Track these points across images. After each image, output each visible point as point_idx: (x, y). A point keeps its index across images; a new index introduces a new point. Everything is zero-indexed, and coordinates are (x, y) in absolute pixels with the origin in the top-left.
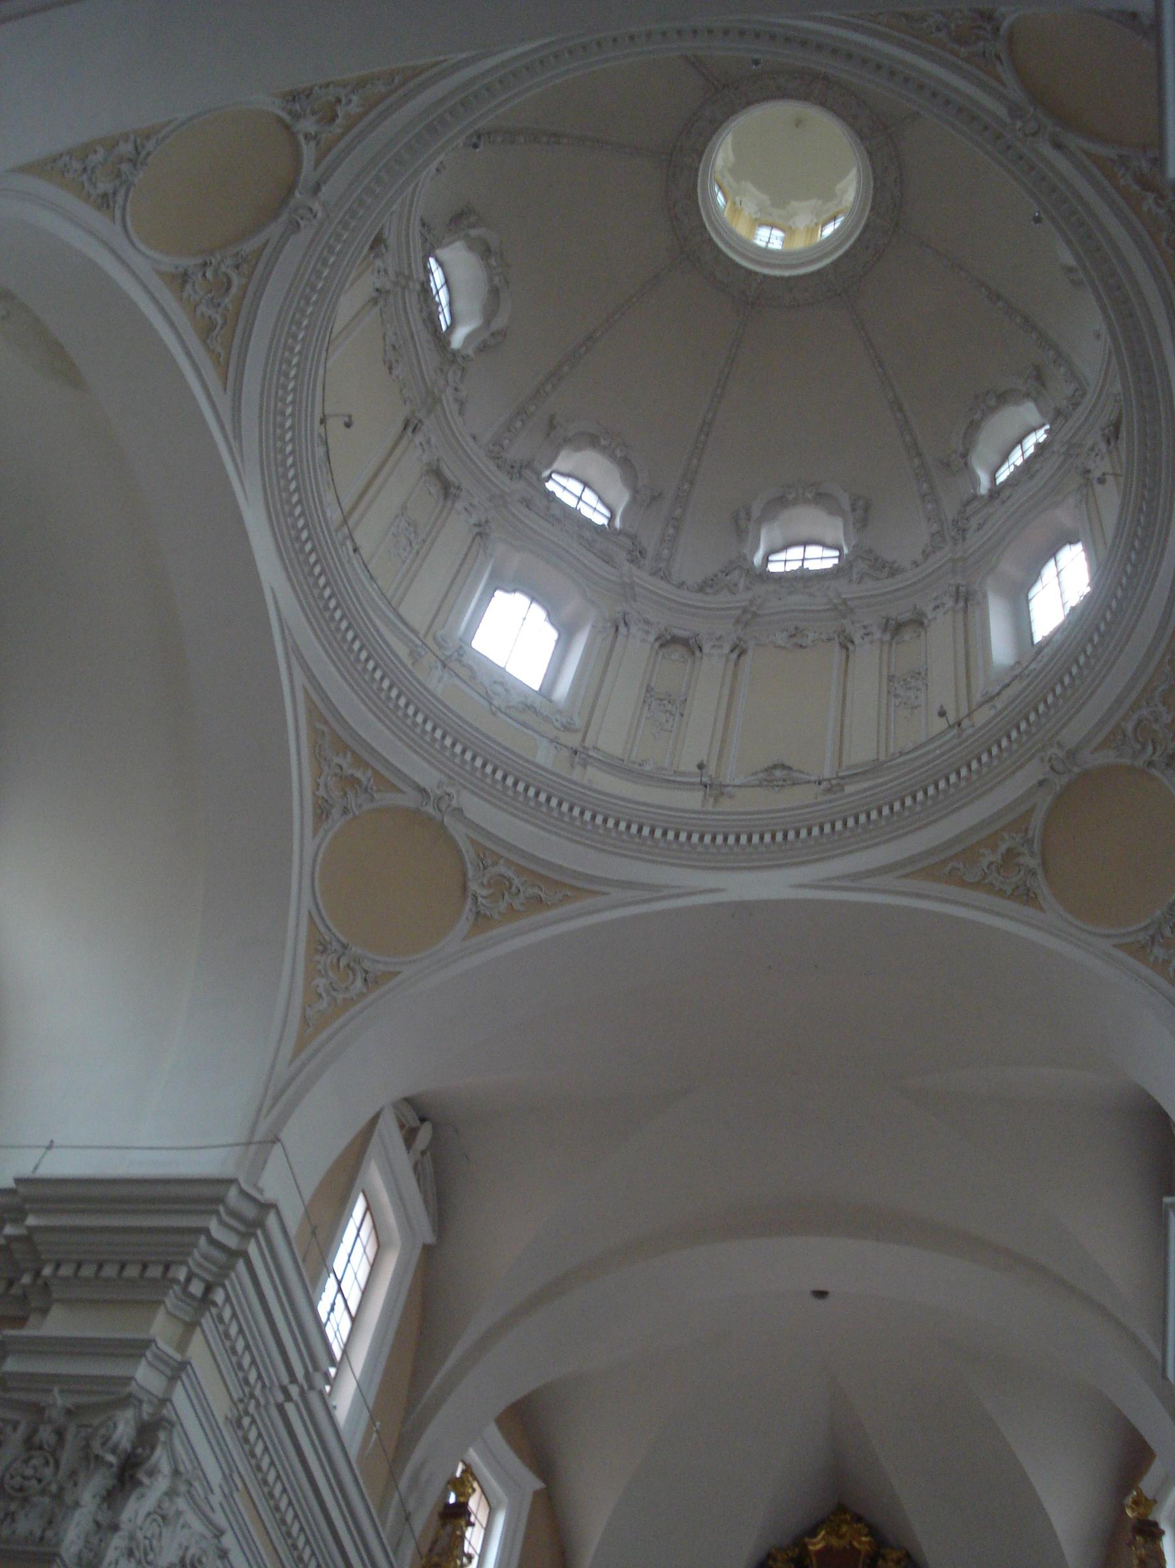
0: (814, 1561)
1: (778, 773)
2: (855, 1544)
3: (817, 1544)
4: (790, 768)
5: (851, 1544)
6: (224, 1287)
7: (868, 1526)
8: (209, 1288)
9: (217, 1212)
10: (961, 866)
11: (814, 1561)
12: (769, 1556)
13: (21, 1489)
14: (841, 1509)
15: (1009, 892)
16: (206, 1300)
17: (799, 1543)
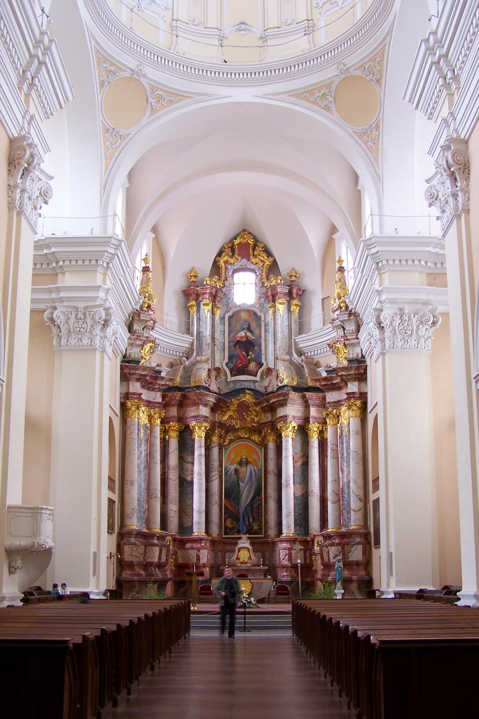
0: (236, 247)
1: (243, 27)
2: (249, 241)
3: (237, 242)
4: (247, 24)
5: (247, 241)
6: (112, 263)
7: (253, 235)
8: (108, 263)
9: (109, 245)
10: (308, 95)
11: (236, 247)
12: (223, 246)
13: (80, 331)
14: (244, 230)
15: (322, 107)
16: (108, 267)
17: (231, 241)
